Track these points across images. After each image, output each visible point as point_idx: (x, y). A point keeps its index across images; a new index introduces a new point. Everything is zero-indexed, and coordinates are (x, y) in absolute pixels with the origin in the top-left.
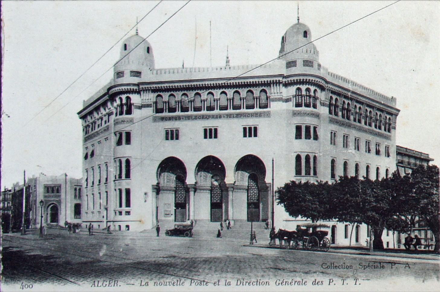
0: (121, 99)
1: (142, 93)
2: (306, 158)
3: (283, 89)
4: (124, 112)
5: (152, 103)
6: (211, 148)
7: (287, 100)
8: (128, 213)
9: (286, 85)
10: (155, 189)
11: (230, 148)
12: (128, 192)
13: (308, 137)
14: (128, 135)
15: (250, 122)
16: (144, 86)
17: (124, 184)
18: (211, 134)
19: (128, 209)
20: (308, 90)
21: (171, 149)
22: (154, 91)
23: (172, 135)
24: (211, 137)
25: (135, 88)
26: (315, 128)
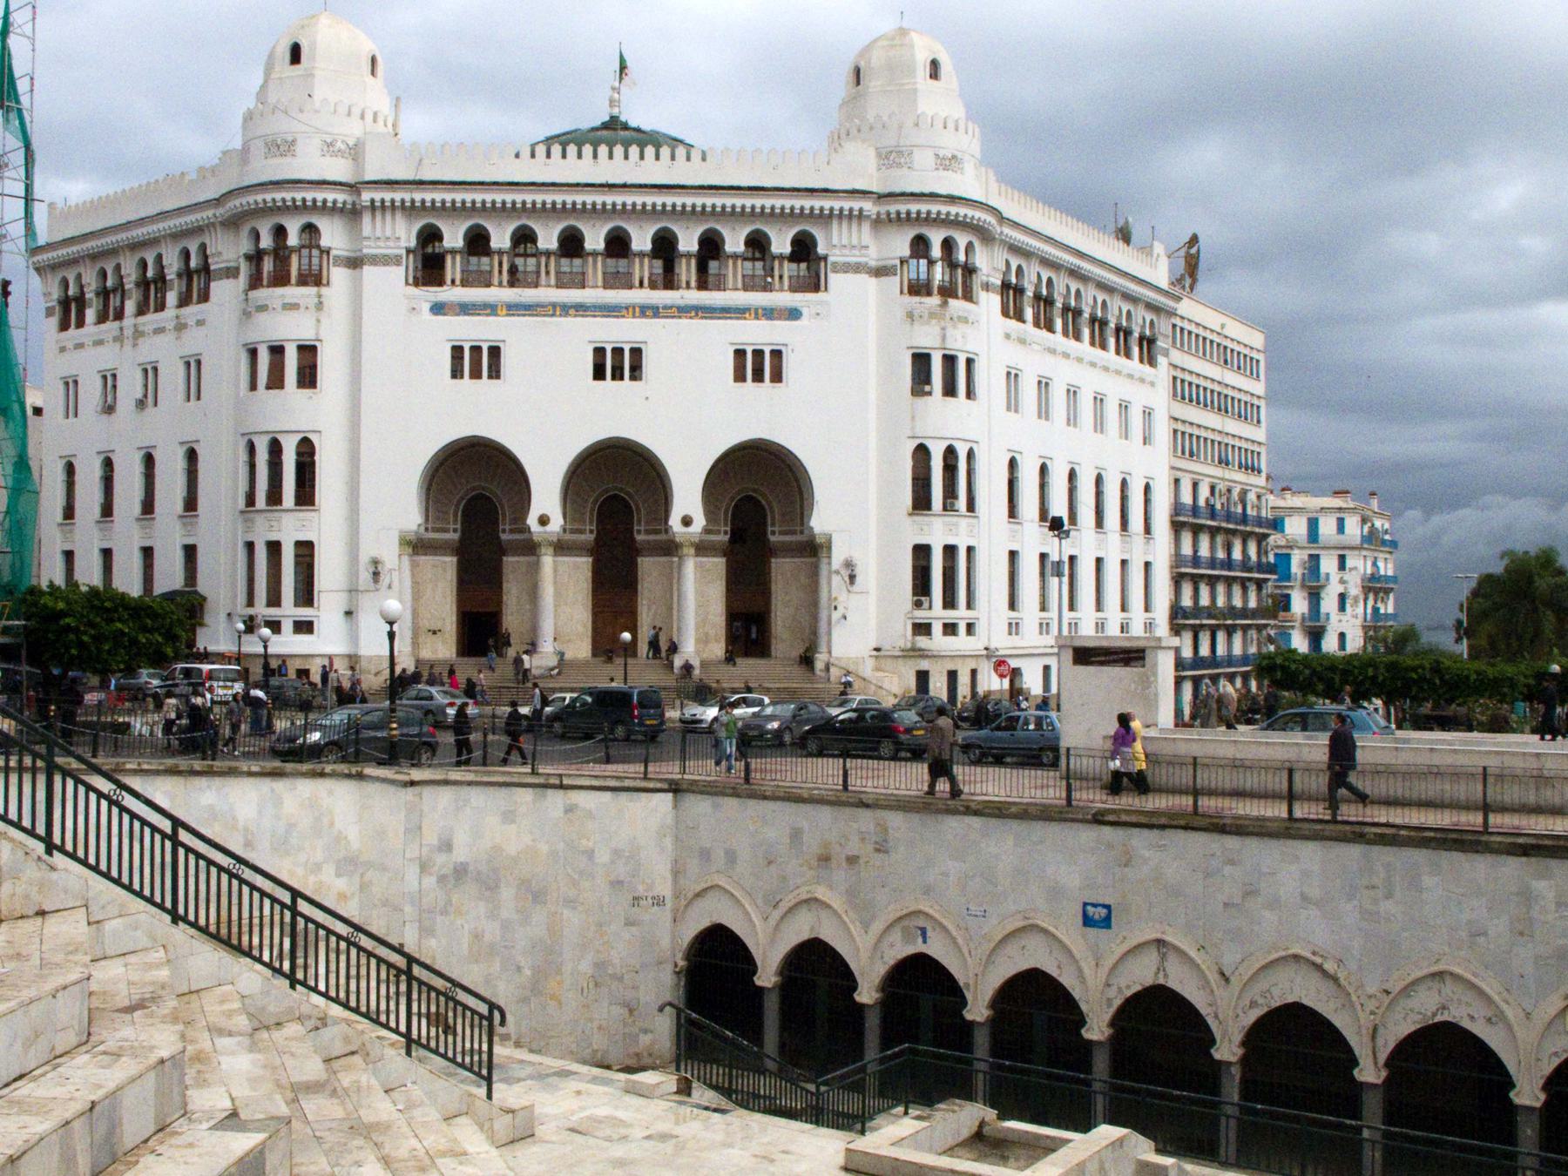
0: (280, 232)
1: (366, 219)
3: (866, 233)
5: (404, 252)
6: (618, 413)
7: (880, 272)
8: (304, 627)
9: (879, 223)
10: (409, 543)
11: (687, 419)
12: (305, 551)
13: (950, 390)
14: (308, 352)
16: (378, 196)
17: (289, 527)
18: (618, 364)
19: (304, 613)
21: (477, 412)
22: (410, 210)
25: (341, 197)
26: (969, 362)
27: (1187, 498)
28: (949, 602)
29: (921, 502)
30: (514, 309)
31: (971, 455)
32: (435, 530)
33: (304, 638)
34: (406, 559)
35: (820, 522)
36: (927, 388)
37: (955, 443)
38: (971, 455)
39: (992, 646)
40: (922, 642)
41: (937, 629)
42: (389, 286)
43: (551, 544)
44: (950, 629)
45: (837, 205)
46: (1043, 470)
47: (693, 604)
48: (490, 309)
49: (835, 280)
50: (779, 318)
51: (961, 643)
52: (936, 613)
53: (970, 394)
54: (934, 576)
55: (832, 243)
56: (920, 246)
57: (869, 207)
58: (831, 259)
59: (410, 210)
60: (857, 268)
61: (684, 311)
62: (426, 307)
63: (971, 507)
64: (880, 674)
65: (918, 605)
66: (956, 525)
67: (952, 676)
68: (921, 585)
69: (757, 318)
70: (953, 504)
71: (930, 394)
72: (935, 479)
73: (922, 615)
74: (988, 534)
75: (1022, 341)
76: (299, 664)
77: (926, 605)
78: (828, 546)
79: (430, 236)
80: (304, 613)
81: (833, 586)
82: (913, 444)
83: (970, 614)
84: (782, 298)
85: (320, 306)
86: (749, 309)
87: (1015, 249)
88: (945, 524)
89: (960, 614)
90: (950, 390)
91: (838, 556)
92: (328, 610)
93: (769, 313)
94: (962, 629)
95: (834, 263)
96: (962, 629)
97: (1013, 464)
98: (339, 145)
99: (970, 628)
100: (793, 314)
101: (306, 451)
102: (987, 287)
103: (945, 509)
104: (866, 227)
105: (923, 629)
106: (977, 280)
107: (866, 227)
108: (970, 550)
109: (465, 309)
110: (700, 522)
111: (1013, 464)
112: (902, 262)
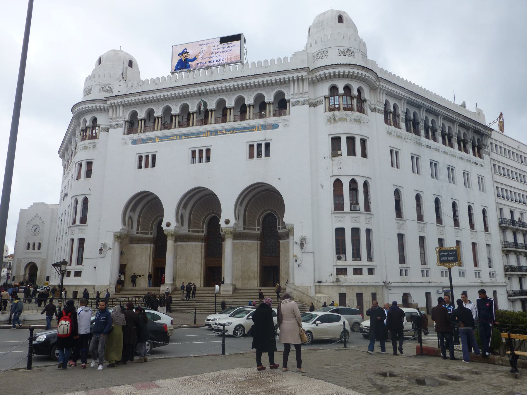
0: (85, 121)
2: (350, 186)
4: (87, 138)
5: (123, 122)
6: (202, 176)
8: (78, 274)
12: (82, 241)
15: (257, 137)
20: (347, 88)
22: (125, 105)
23: (147, 161)
27: (508, 216)
28: (357, 255)
30: (161, 138)
31: (366, 184)
32: (141, 233)
33: (78, 278)
34: (116, 244)
36: (339, 152)
37: (356, 178)
38: (366, 184)
39: (388, 281)
40: (341, 277)
41: (350, 271)
42: (118, 134)
43: (172, 235)
44: (357, 271)
45: (291, 76)
46: (418, 198)
47: (239, 262)
48: (152, 140)
49: (293, 110)
50: (269, 129)
51: (365, 279)
52: (349, 262)
53: (364, 154)
54: (349, 244)
56: (334, 89)
57: (305, 74)
58: (291, 101)
59: (125, 105)
60: (303, 103)
62: (131, 141)
63: (368, 208)
64: (319, 295)
65: (339, 258)
66: (359, 217)
67: (360, 297)
68: (340, 249)
69: (259, 130)
70: (355, 207)
71: (341, 155)
73: (341, 264)
74: (383, 224)
75: (400, 137)
76: (73, 289)
77: (343, 259)
79: (134, 115)
80: (79, 268)
82: (334, 179)
83: (370, 263)
84: (271, 120)
85: (94, 147)
86: (256, 127)
87: (389, 94)
88: (352, 217)
89: (364, 262)
91: (296, 236)
92: (86, 267)
93: (265, 127)
94: (365, 271)
95: (293, 102)
96: (365, 271)
97: (397, 193)
98: (107, 88)
99: (371, 271)
100: (275, 126)
101: (86, 201)
102: (374, 110)
103: (351, 210)
104: (306, 84)
105: (342, 271)
106: (366, 106)
107: (306, 84)
108: (368, 231)
109: (144, 141)
110: (233, 221)
111: (397, 193)
112: (325, 98)
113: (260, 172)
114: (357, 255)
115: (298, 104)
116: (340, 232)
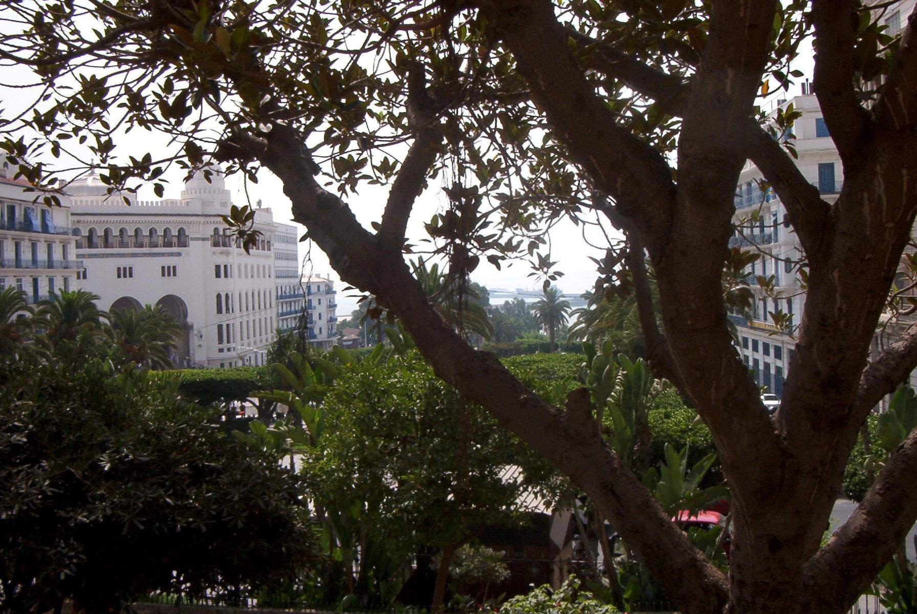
11: (147, 289)
18: (125, 273)
24: (125, 276)
28: (228, 342)
29: (219, 311)
35: (190, 320)
44: (229, 350)
49: (191, 243)
55: (190, 232)
57: (202, 219)
61: (145, 255)
67: (231, 364)
72: (222, 304)
73: (221, 346)
74: (236, 319)
78: (192, 327)
81: (194, 341)
89: (232, 345)
90: (226, 276)
93: (171, 254)
100: (179, 254)
113: (169, 287)
114: (228, 342)
115: (193, 239)
116: (220, 327)
